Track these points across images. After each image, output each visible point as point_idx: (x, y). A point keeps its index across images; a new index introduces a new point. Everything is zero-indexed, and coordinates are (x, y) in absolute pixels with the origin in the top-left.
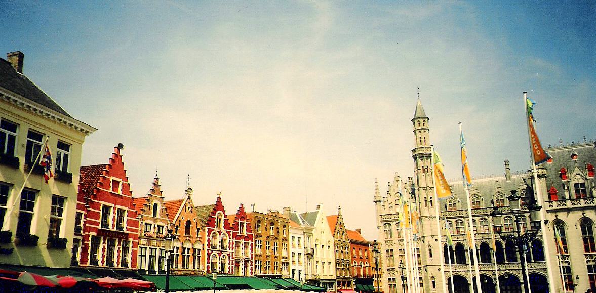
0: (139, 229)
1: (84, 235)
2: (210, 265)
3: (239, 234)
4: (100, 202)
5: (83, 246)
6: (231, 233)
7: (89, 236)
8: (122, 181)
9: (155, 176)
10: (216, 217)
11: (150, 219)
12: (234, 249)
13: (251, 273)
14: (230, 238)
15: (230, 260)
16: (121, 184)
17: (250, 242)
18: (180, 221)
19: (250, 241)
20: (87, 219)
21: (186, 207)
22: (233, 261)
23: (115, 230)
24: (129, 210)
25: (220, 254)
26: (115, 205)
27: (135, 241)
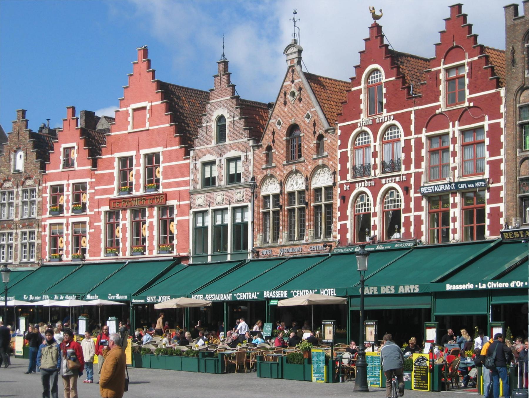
0: (191, 177)
1: (93, 213)
2: (349, 223)
3: (443, 109)
4: (113, 156)
5: (93, 230)
6: (413, 116)
7: (99, 213)
8: (150, 104)
9: (219, 59)
10: (362, 86)
11: (210, 152)
12: (423, 164)
13: (495, 227)
14: (408, 133)
15: (408, 200)
16: (148, 108)
17: (486, 123)
18: (274, 133)
19: (487, 117)
20: (96, 188)
21: (285, 94)
22: (418, 201)
23: (141, 192)
24: (165, 149)
25: (375, 190)
26: (138, 151)
27: (181, 203)
